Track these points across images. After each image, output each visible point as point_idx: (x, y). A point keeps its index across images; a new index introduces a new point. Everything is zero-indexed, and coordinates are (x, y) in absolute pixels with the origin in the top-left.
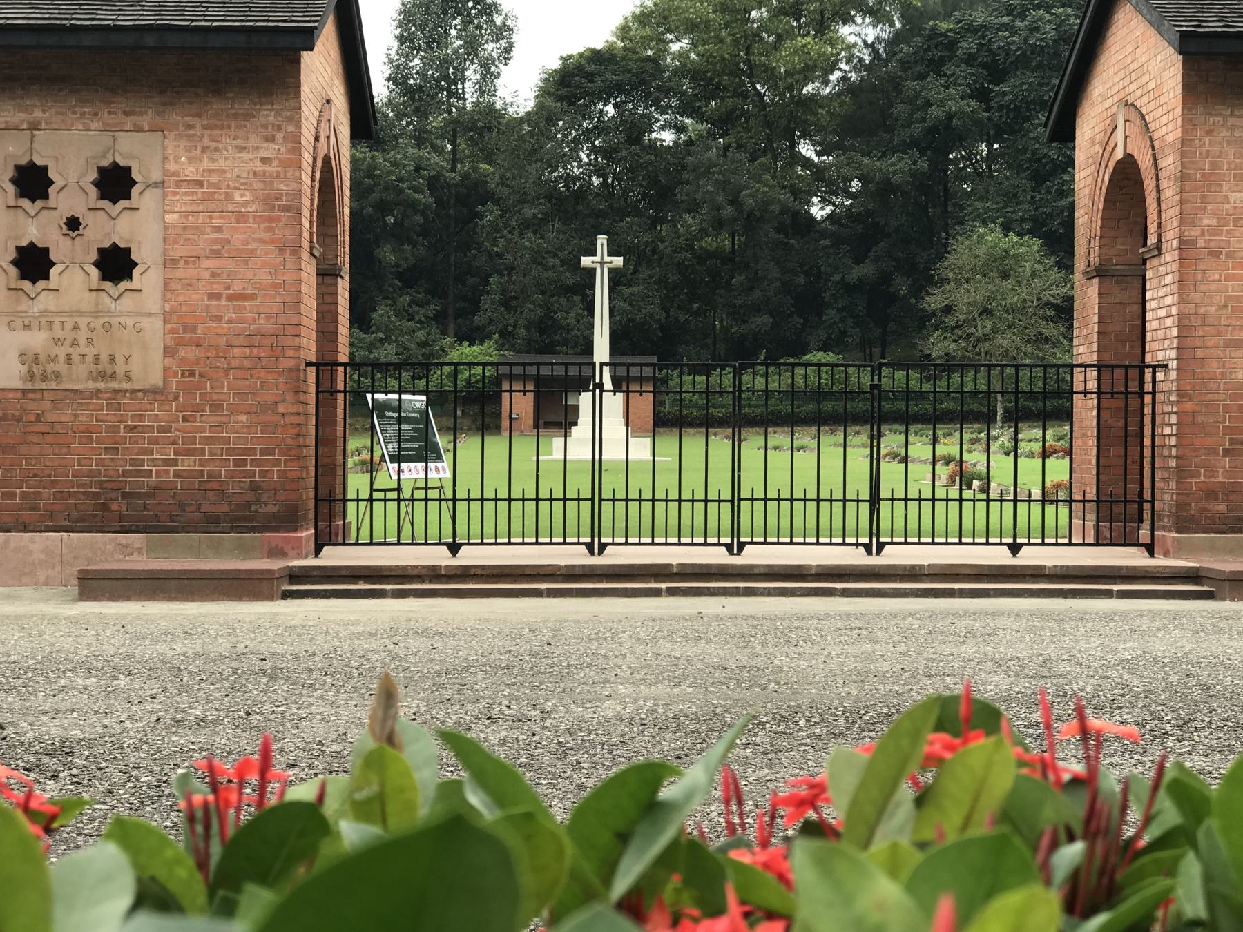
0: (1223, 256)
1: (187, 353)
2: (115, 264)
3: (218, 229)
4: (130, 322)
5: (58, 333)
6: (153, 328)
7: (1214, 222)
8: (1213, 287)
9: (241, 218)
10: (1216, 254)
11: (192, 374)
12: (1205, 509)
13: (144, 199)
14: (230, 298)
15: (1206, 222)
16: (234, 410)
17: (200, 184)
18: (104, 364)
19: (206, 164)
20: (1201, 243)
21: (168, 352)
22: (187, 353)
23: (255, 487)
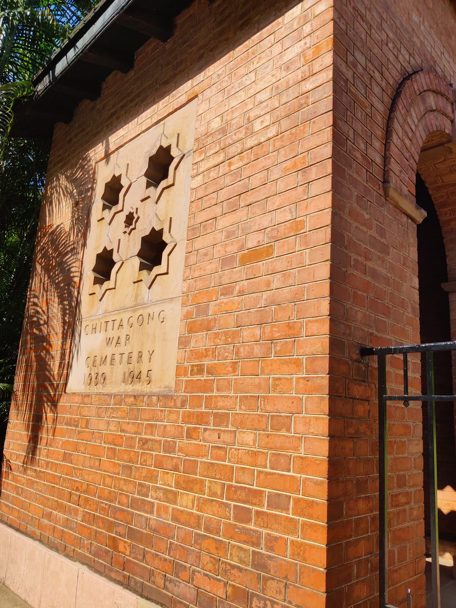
1: (200, 341)
2: (153, 249)
4: (156, 310)
6: (174, 313)
11: (200, 370)
13: (182, 176)
14: (244, 261)
16: (241, 424)
18: (134, 366)
21: (183, 342)
22: (200, 341)
23: (259, 563)
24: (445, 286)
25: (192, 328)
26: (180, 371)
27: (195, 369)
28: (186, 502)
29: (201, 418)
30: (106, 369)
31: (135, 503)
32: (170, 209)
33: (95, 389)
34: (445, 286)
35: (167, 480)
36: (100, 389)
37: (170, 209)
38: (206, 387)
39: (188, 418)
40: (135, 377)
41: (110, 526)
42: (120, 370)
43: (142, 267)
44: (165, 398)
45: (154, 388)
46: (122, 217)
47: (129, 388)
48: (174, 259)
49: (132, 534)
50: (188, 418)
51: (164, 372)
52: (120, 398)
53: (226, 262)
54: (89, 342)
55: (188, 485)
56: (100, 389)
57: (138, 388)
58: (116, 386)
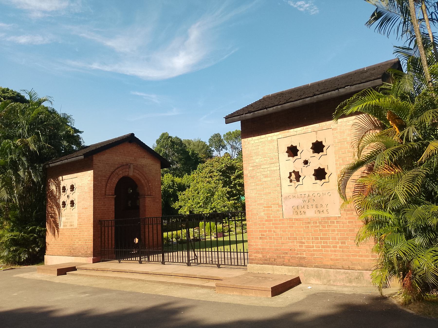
0: (255, 178)
3: (83, 195)
4: (74, 214)
5: (67, 218)
6: (76, 215)
7: (251, 168)
8: (253, 187)
9: (86, 193)
10: (253, 177)
12: (256, 256)
13: (76, 190)
15: (250, 169)
17: (81, 186)
18: (71, 224)
19: (83, 183)
20: (249, 175)
21: (78, 220)
24: (139, 197)
25: (79, 218)
26: (78, 225)
27: (79, 224)
28: (80, 243)
29: (81, 231)
30: (66, 224)
31: (73, 245)
32: (74, 196)
33: (65, 228)
34: (139, 197)
35: (77, 240)
36: (66, 228)
37: (74, 196)
38: (81, 227)
39: (79, 231)
40: (71, 225)
41: (70, 249)
42: (68, 225)
43: (71, 206)
44: (76, 229)
45: (74, 227)
46: (66, 195)
47: (71, 227)
48: (76, 205)
49: (73, 249)
50: (79, 231)
51: (76, 225)
52: (69, 229)
53: (83, 209)
54: (63, 219)
55: (80, 240)
56: (66, 228)
57: (72, 227)
58: (68, 227)
